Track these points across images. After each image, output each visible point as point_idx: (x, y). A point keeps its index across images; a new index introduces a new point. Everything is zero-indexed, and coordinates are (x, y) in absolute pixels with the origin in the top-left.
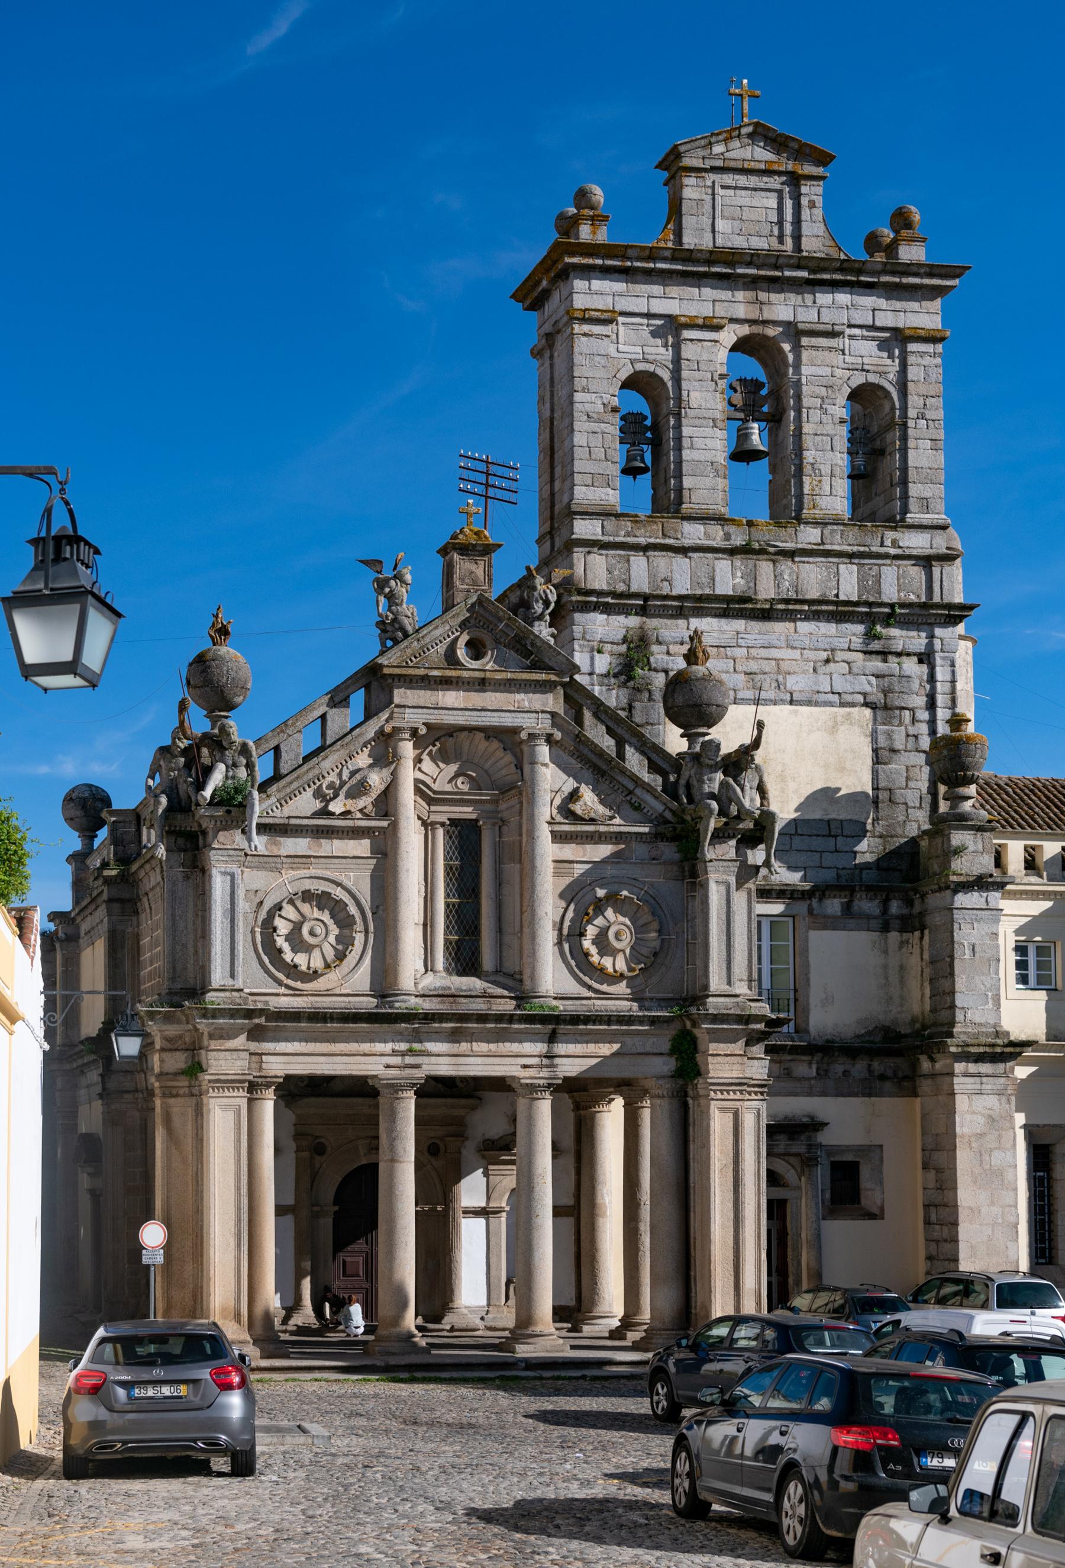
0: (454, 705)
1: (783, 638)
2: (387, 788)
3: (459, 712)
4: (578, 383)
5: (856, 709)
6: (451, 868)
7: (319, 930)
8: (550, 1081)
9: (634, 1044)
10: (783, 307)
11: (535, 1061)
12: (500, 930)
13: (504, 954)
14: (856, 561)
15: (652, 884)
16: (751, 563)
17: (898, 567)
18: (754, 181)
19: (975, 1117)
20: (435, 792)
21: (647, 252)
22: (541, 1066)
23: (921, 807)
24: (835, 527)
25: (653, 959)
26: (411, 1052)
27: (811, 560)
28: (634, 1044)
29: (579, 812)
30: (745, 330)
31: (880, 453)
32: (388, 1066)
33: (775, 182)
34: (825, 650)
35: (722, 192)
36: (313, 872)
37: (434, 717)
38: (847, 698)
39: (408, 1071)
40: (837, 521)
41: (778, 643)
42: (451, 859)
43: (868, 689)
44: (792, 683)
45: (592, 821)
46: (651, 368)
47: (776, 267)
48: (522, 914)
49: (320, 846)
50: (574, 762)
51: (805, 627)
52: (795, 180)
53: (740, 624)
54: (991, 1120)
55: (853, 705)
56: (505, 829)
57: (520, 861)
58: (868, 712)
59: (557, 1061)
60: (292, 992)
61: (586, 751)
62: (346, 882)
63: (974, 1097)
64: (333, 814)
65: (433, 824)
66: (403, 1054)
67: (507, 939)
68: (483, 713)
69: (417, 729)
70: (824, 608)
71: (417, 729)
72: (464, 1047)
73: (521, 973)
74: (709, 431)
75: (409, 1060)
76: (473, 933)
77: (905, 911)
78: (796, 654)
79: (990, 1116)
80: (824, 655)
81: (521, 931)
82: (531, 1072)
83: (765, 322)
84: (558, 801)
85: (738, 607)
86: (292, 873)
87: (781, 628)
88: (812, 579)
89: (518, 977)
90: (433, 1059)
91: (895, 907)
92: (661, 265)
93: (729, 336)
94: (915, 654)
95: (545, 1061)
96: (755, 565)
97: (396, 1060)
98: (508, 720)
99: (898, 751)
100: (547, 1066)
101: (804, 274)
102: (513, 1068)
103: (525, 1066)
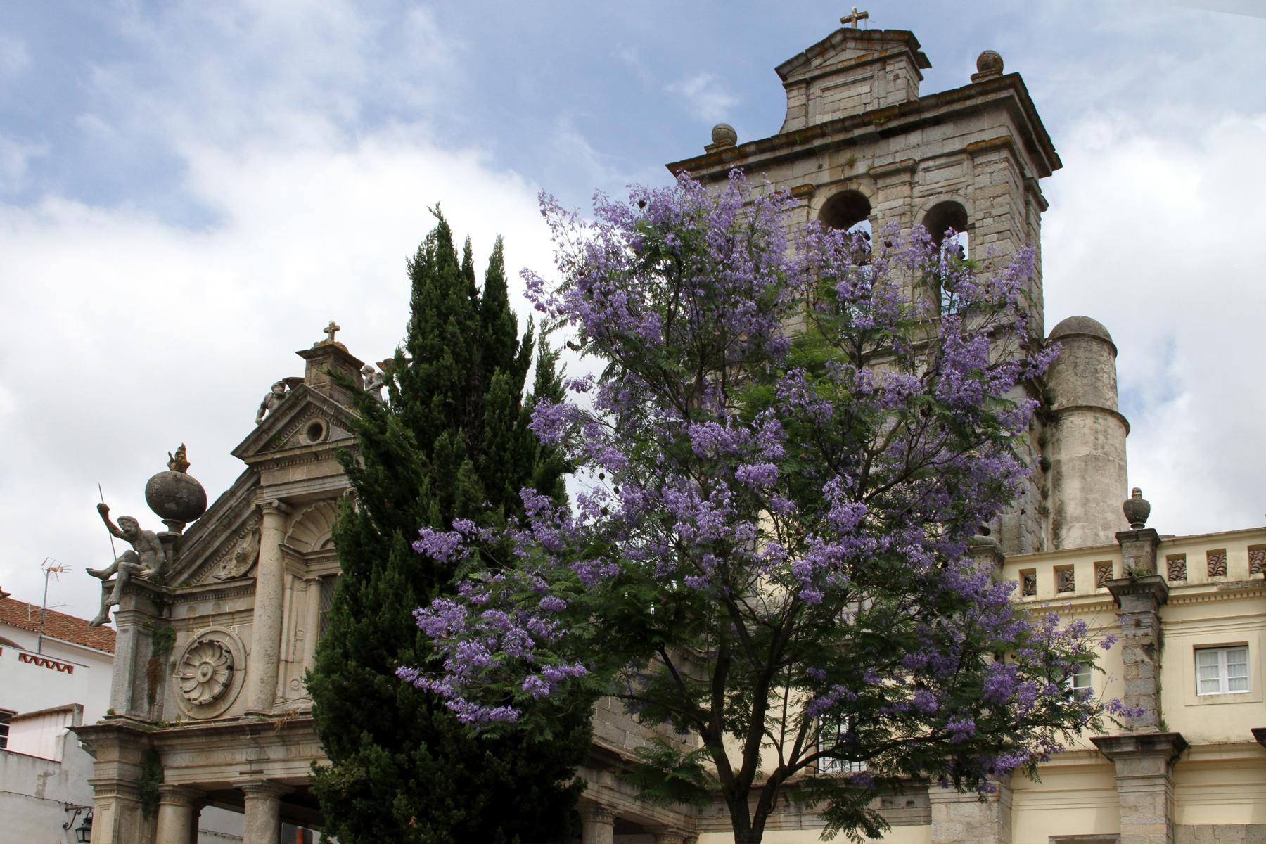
19: (952, 824)
26: (259, 761)
47: (846, 130)
54: (970, 826)
62: (233, 634)
63: (952, 806)
65: (307, 581)
66: (250, 762)
72: (294, 750)
75: (255, 767)
79: (969, 824)
83: (850, 179)
97: (246, 768)
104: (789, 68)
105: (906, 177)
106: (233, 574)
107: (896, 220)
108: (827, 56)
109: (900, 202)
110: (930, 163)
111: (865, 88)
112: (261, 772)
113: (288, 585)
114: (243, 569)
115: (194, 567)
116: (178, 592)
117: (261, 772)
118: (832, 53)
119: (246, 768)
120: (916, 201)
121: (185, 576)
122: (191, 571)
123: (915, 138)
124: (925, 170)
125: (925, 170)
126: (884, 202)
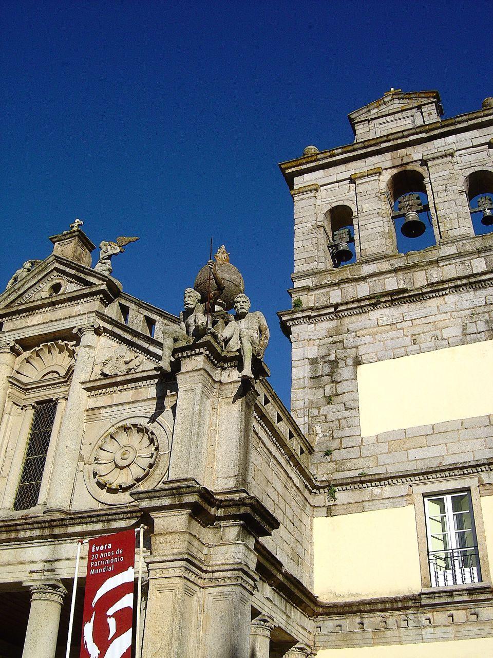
0: (35, 325)
1: (436, 309)
3: (36, 327)
4: (296, 221)
10: (416, 153)
11: (39, 567)
14: (483, 255)
16: (409, 275)
20: (26, 385)
22: (43, 571)
24: (465, 242)
25: (147, 469)
27: (451, 262)
29: (107, 371)
30: (395, 171)
33: (409, 113)
34: (469, 309)
35: (381, 126)
37: (20, 335)
40: (465, 237)
41: (433, 313)
44: (446, 333)
45: (116, 375)
51: (451, 299)
53: (405, 308)
59: (57, 565)
68: (51, 324)
70: (459, 283)
74: (377, 219)
78: (448, 316)
80: (469, 312)
82: (37, 576)
85: (397, 297)
87: (432, 304)
88: (450, 271)
93: (386, 176)
95: (47, 566)
96: (413, 275)
98: (67, 324)
100: (48, 571)
101: (423, 135)
102: (23, 574)
103: (32, 572)
105: (450, 158)
107: (446, 182)
108: (380, 109)
110: (464, 151)
111: (409, 121)
113: (7, 411)
120: (456, 172)
123: (451, 139)
124: (461, 155)
125: (461, 155)
126: (435, 177)
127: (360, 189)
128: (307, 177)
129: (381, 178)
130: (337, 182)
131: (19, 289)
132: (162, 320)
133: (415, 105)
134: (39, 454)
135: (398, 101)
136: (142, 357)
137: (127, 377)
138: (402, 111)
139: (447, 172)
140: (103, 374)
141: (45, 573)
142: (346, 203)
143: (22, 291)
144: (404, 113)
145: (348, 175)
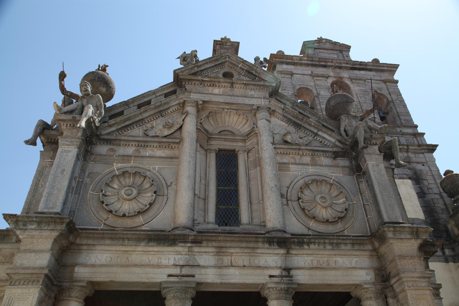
2: (181, 128)
5: (405, 180)
6: (221, 173)
7: (130, 192)
8: (289, 286)
9: (344, 262)
11: (276, 272)
12: (250, 202)
13: (254, 215)
15: (336, 177)
17: (405, 137)
18: (329, 52)
21: (299, 58)
22: (282, 276)
23: (443, 213)
25: (345, 212)
28: (344, 262)
29: (289, 140)
30: (335, 79)
31: (387, 114)
32: (170, 276)
33: (335, 52)
36: (132, 164)
38: (401, 176)
39: (185, 279)
42: (221, 168)
43: (407, 173)
46: (305, 86)
48: (262, 189)
49: (140, 153)
50: (284, 123)
52: (341, 51)
55: (404, 179)
56: (250, 154)
57: (260, 165)
58: (410, 181)
60: (108, 228)
61: (289, 116)
64: (148, 136)
67: (255, 207)
69: (197, 102)
71: (197, 102)
73: (264, 222)
75: (185, 271)
76: (221, 173)
77: (453, 254)
81: (263, 200)
84: (278, 138)
86: (120, 165)
89: (262, 224)
90: (203, 271)
91: (447, 252)
92: (303, 62)
94: (421, 163)
95: (284, 273)
99: (427, 193)
100: (286, 276)
103: (271, 276)
104: (308, 43)
105: (363, 82)
106: (157, 134)
107: (364, 93)
109: (364, 88)
111: (335, 56)
112: (193, 276)
114: (166, 132)
115: (123, 125)
116: (106, 137)
117: (193, 276)
118: (322, 44)
119: (176, 271)
121: (113, 129)
122: (120, 127)
123: (363, 72)
127: (318, 82)
128: (285, 66)
129: (328, 80)
130: (302, 75)
131: (200, 66)
132: (314, 117)
133: (338, 49)
134: (226, 186)
135: (329, 44)
136: (311, 138)
137: (308, 148)
138: (331, 50)
139: (364, 88)
140: (286, 142)
141: (285, 279)
142: (309, 87)
143: (203, 68)
144: (332, 52)
145: (310, 72)
